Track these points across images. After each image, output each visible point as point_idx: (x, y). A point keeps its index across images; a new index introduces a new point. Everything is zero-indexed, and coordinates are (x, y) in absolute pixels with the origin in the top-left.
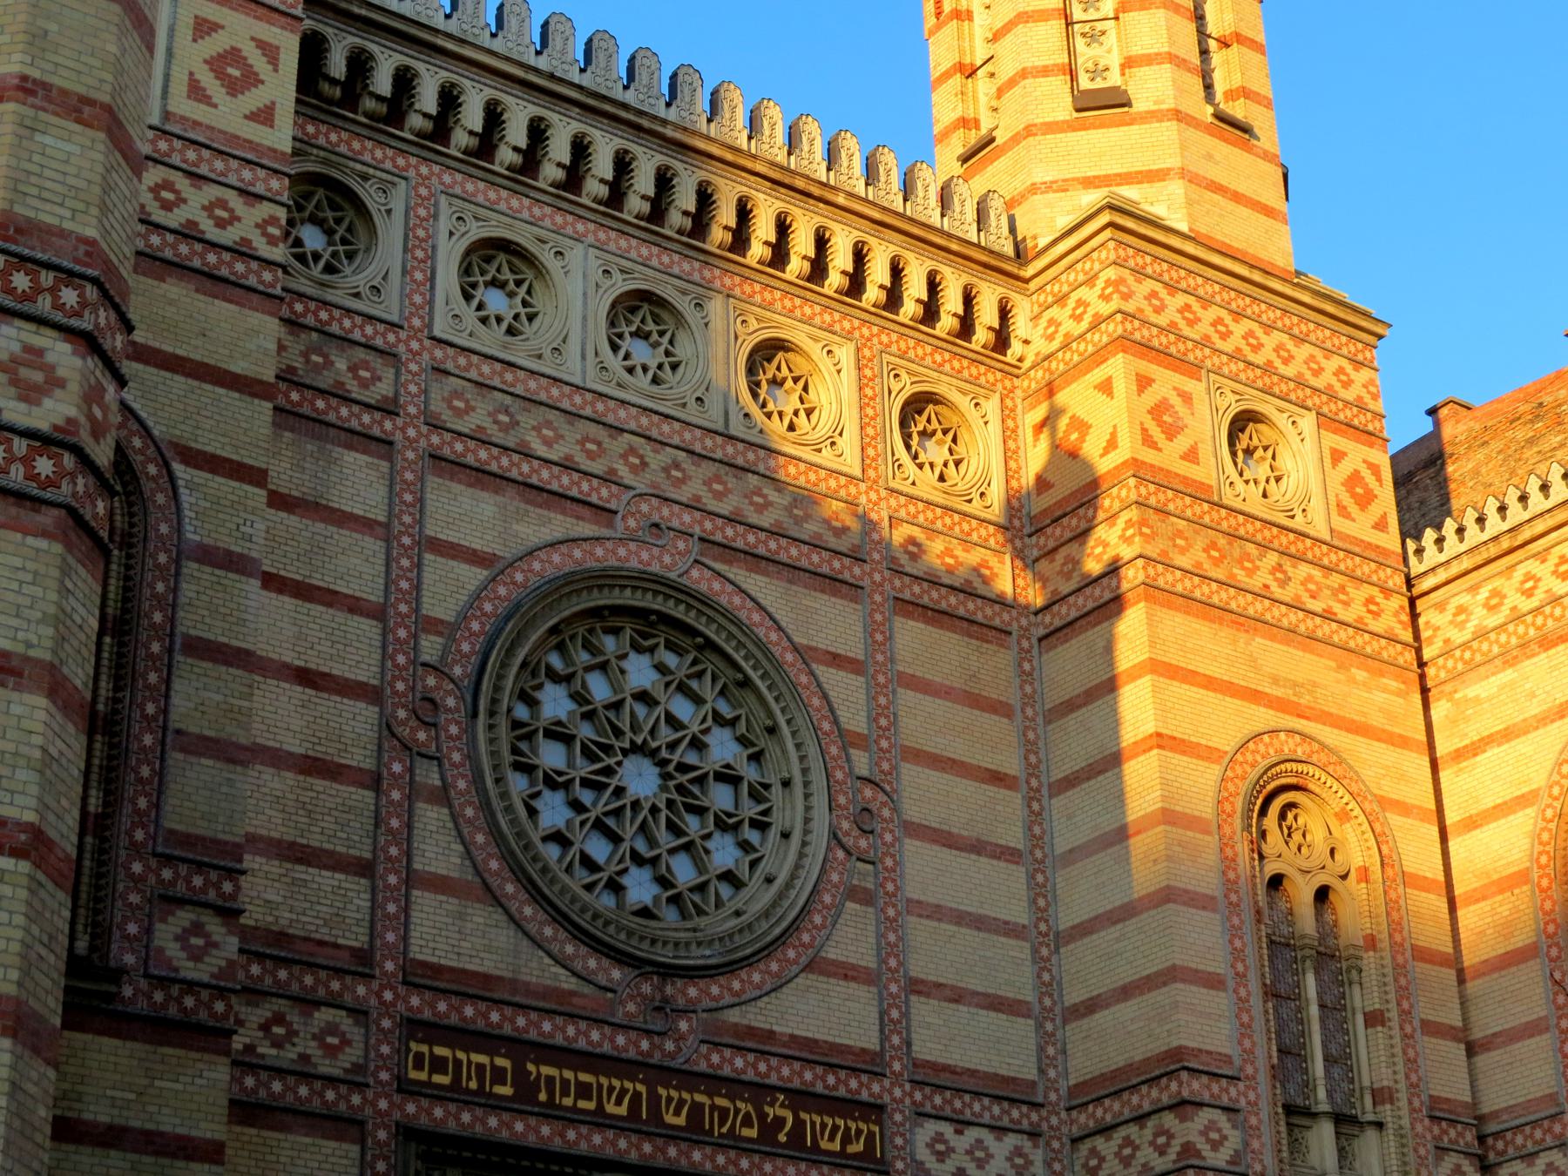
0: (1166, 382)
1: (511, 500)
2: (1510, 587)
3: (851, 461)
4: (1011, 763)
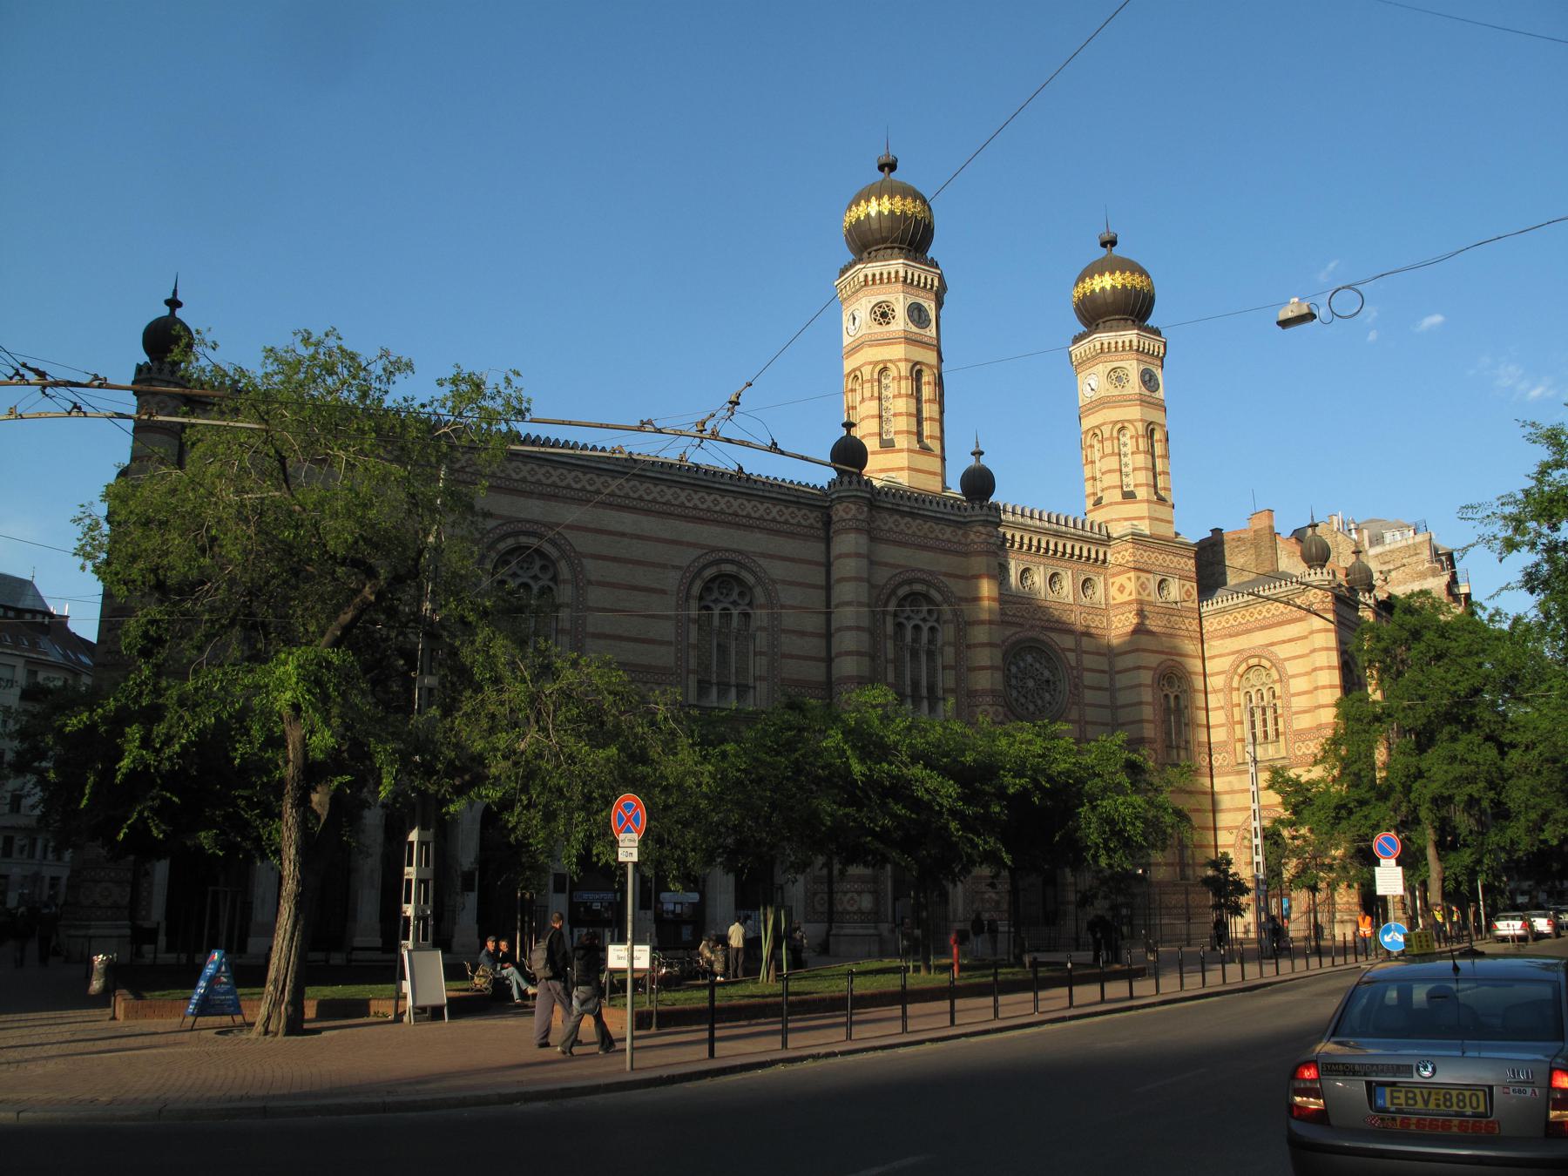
0: (1144, 576)
2: (1223, 620)
4: (1106, 668)
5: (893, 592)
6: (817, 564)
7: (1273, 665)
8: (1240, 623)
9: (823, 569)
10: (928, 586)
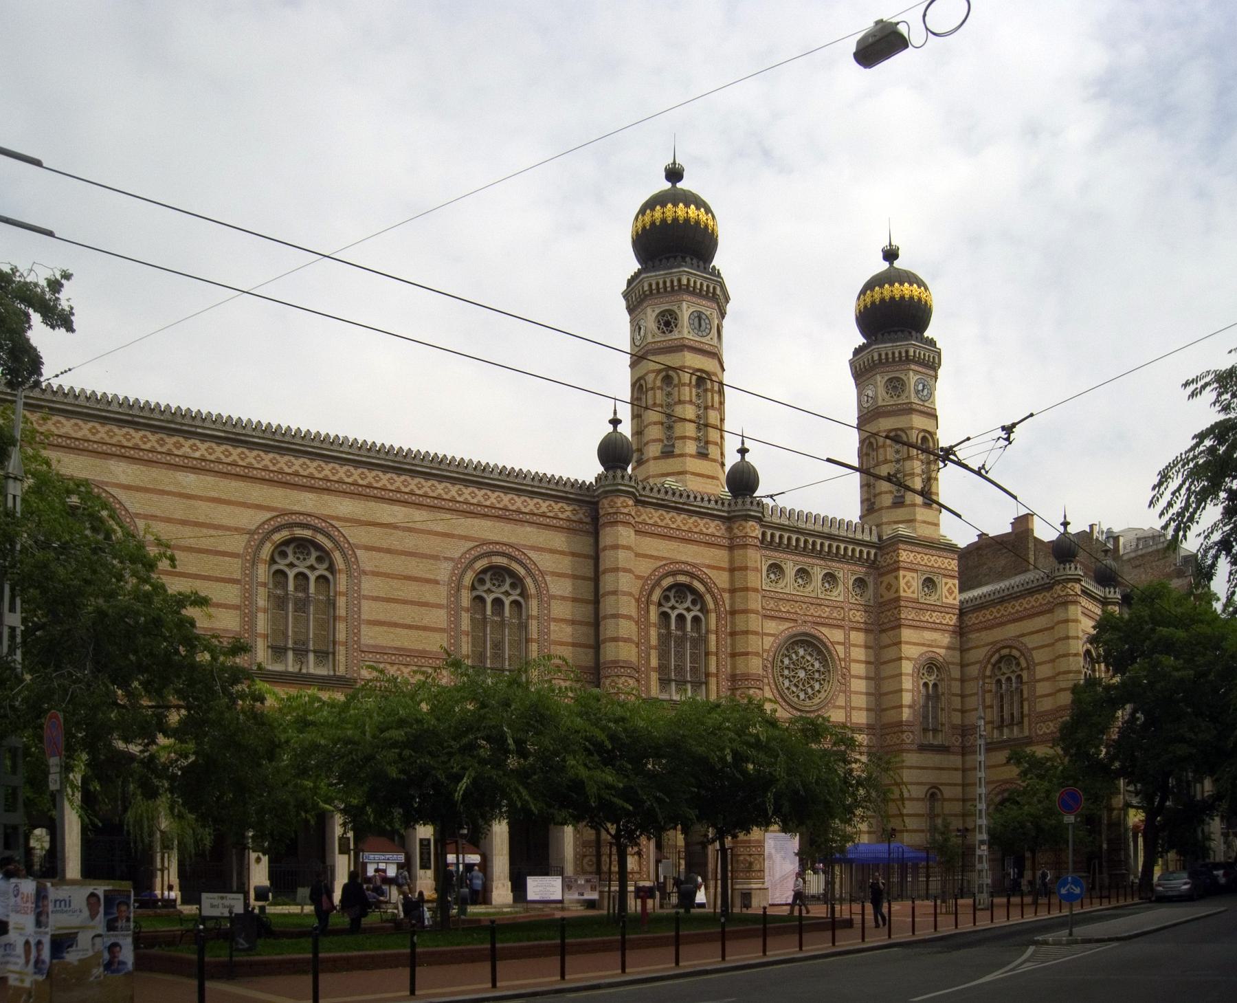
0: (909, 575)
1: (778, 621)
3: (841, 599)
5: (658, 583)
6: (586, 556)
7: (1022, 654)
8: (996, 618)
9: (591, 562)
10: (692, 577)
